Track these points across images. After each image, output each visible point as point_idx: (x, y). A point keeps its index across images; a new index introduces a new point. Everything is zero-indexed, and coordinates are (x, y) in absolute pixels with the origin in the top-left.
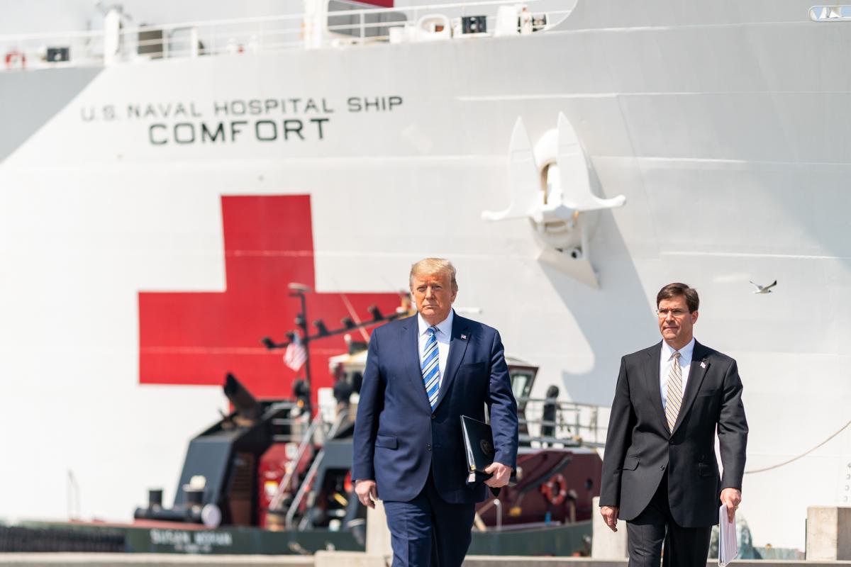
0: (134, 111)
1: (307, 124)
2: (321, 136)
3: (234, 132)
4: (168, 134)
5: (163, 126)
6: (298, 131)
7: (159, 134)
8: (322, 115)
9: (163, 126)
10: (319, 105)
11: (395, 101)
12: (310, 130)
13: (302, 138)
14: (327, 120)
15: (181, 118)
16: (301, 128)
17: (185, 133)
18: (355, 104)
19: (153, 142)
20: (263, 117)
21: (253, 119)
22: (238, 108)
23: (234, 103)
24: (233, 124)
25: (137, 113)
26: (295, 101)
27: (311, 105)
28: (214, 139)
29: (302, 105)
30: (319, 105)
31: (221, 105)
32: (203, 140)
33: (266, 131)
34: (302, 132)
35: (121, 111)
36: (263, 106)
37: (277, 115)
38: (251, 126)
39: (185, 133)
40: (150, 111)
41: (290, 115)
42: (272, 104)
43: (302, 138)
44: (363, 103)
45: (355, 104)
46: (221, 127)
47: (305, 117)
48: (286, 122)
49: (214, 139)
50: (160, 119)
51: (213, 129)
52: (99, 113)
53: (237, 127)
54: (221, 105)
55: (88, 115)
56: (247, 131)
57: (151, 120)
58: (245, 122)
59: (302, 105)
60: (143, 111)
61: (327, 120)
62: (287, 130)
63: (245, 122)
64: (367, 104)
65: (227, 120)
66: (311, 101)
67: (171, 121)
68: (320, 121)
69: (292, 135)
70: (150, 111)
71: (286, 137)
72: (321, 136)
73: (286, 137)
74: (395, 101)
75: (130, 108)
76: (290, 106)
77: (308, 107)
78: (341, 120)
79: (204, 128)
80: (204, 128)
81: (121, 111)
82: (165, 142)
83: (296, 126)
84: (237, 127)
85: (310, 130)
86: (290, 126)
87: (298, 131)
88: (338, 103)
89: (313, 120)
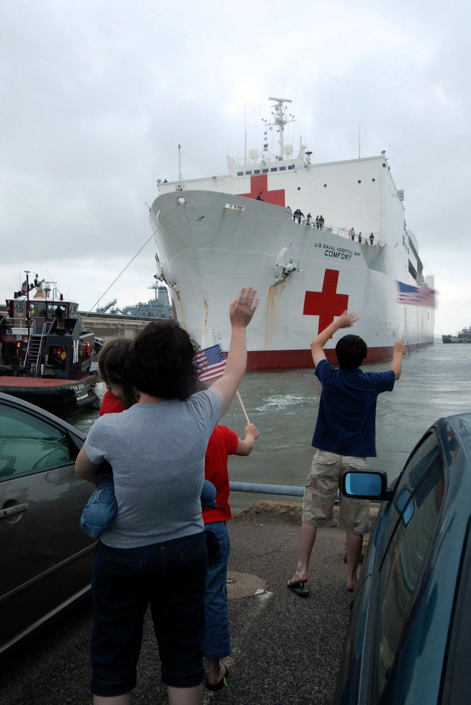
3: (339, 255)
5: (328, 251)
7: (327, 253)
9: (328, 251)
12: (349, 257)
15: (332, 250)
17: (331, 254)
18: (356, 254)
19: (325, 255)
20: (343, 253)
21: (342, 253)
24: (339, 253)
26: (348, 250)
29: (349, 252)
37: (345, 253)
39: (331, 253)
45: (356, 254)
47: (349, 254)
50: (328, 250)
51: (335, 254)
55: (316, 245)
57: (327, 249)
58: (340, 254)
62: (346, 257)
63: (340, 254)
67: (330, 250)
68: (350, 256)
78: (353, 256)
80: (334, 253)
81: (322, 246)
82: (327, 255)
87: (347, 257)
88: (353, 253)
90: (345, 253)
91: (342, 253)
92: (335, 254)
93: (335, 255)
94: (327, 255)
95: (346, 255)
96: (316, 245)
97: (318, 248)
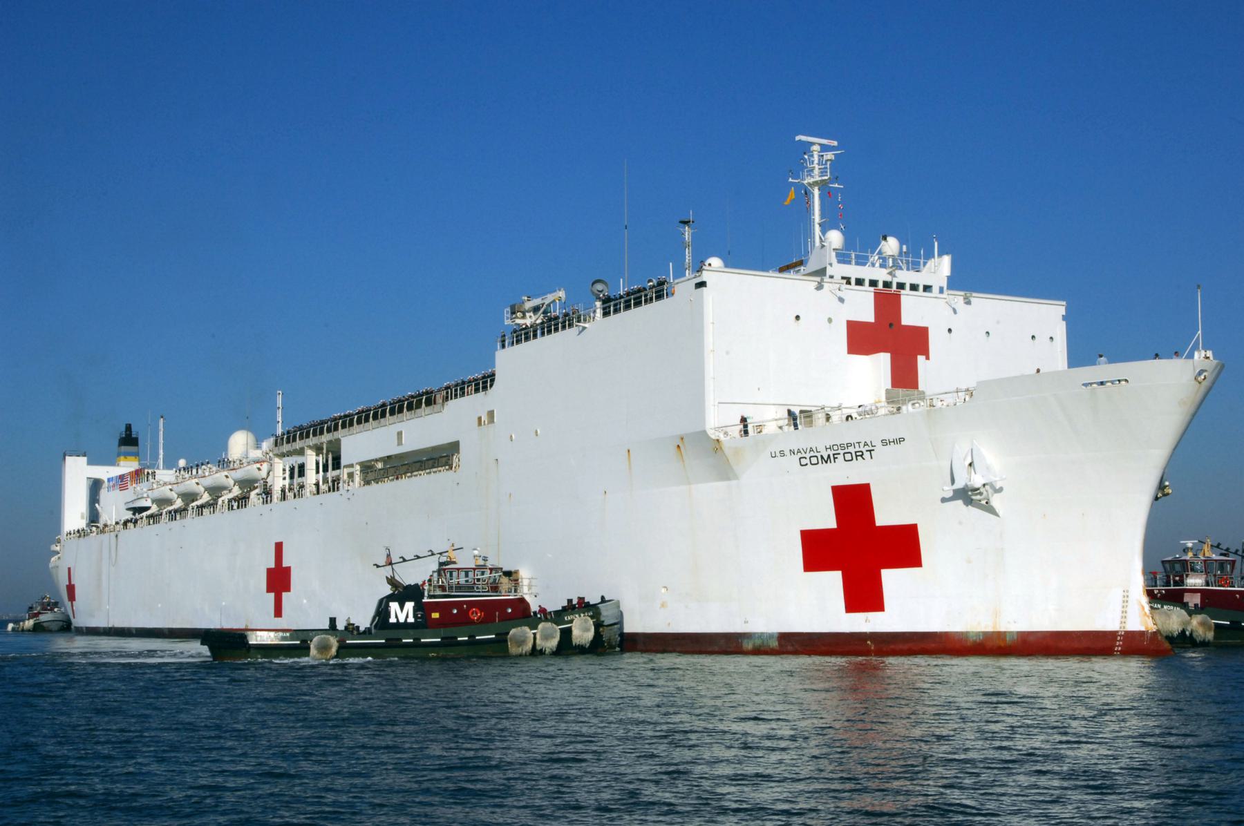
0: (791, 452)
1: (865, 452)
2: (871, 458)
3: (835, 458)
4: (807, 461)
6: (861, 456)
8: (871, 448)
10: (870, 445)
11: (901, 440)
12: (867, 455)
13: (864, 459)
14: (873, 450)
15: (812, 454)
16: (863, 454)
17: (814, 460)
18: (885, 443)
20: (846, 451)
21: (842, 452)
22: (835, 448)
23: (833, 446)
24: (834, 455)
25: (794, 453)
26: (859, 443)
27: (866, 444)
28: (826, 462)
29: (862, 445)
30: (870, 444)
31: (828, 447)
32: (822, 463)
33: (848, 457)
34: (863, 456)
35: (787, 452)
36: (845, 446)
37: (851, 449)
38: (842, 455)
39: (814, 460)
40: (799, 451)
41: (857, 449)
42: (849, 445)
43: (864, 459)
44: (888, 442)
45: (885, 443)
46: (829, 456)
47: (862, 449)
48: (856, 452)
49: (826, 462)
50: (804, 455)
51: (826, 459)
52: (778, 454)
53: (836, 456)
54: (828, 447)
56: (840, 457)
57: (800, 456)
58: (839, 454)
59: (862, 445)
60: (796, 453)
61: (873, 450)
62: (857, 456)
63: (839, 454)
64: (890, 442)
65: (831, 453)
66: (865, 442)
67: (808, 456)
68: (870, 451)
69: (859, 458)
70: (799, 451)
71: (857, 459)
72: (871, 458)
73: (857, 459)
74: (901, 440)
75: (790, 450)
76: (857, 445)
77: (865, 445)
78: (879, 449)
79: (822, 457)
81: (787, 452)
82: (807, 464)
83: (861, 453)
84: (836, 456)
85: (867, 455)
86: (858, 454)
87: (861, 456)
89: (867, 451)
90: (851, 449)
91: (842, 452)
92: (826, 459)
93: (826, 460)
94: (807, 464)
95: (856, 452)
96: (773, 456)
97: (779, 459)
